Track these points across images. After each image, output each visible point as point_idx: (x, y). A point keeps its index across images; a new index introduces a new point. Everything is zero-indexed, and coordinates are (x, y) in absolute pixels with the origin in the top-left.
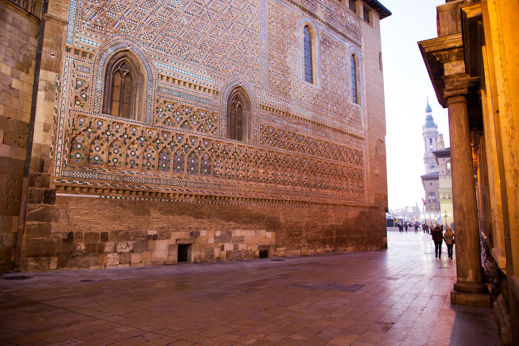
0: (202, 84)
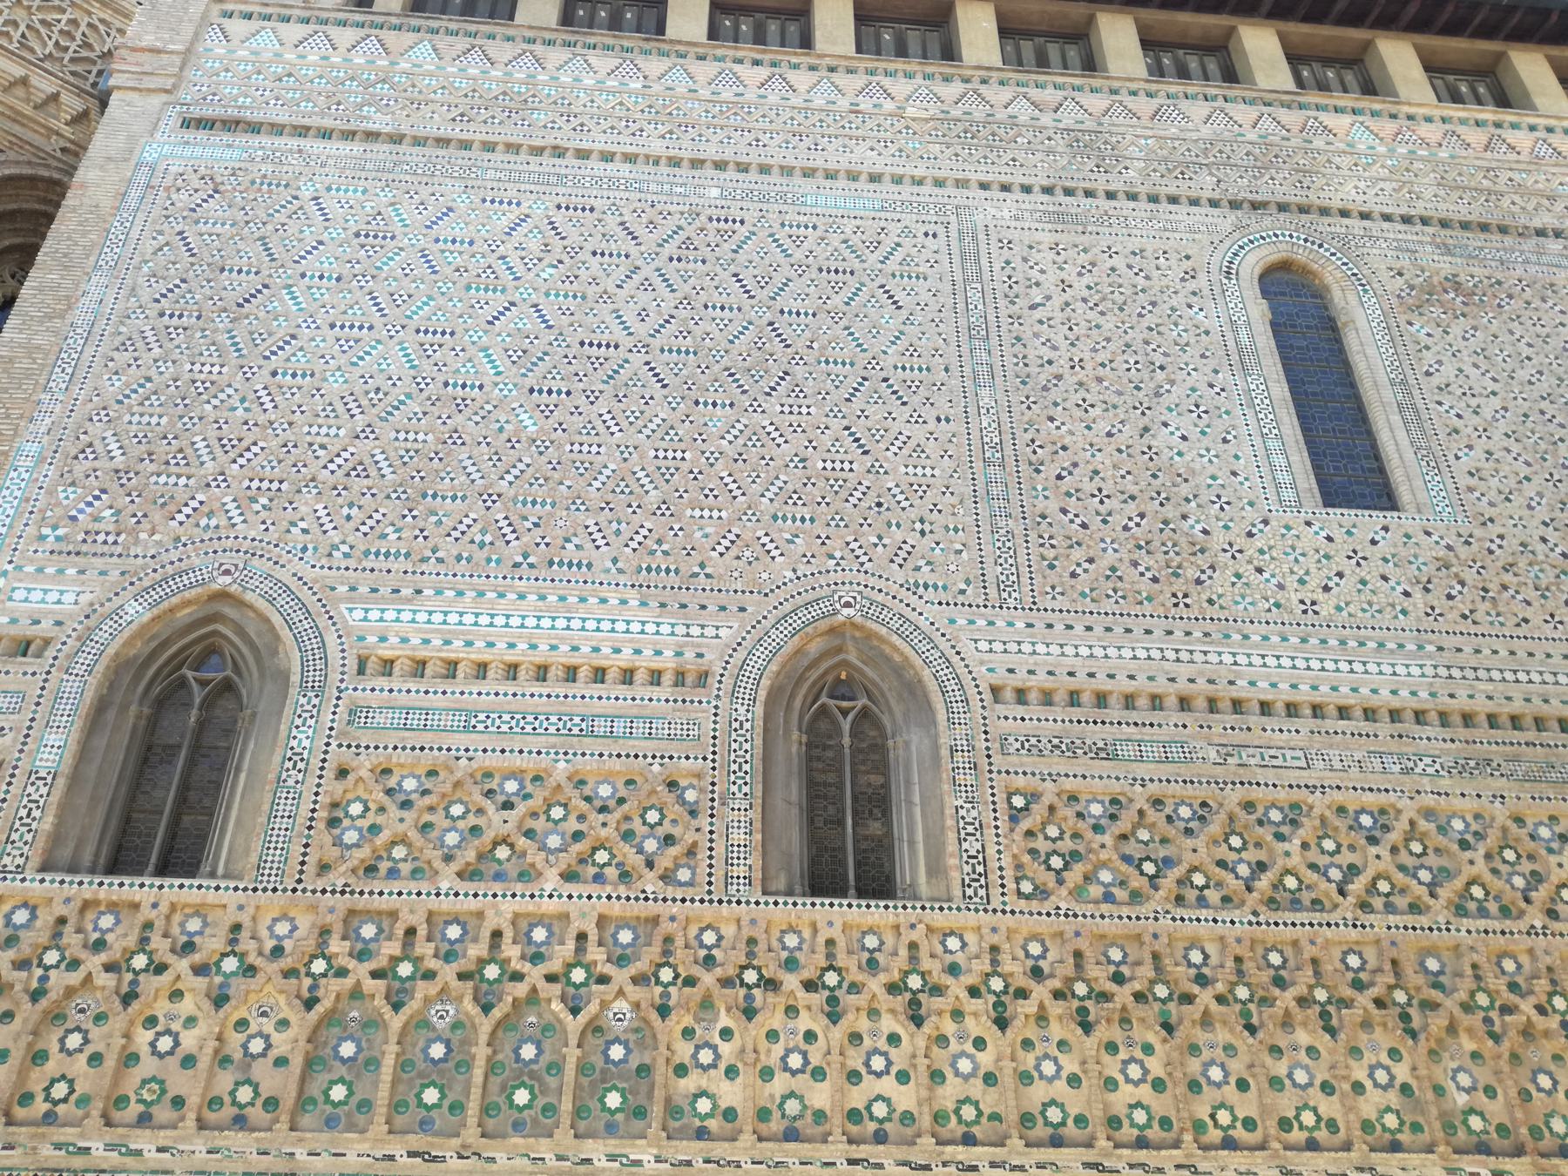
0: (606, 650)
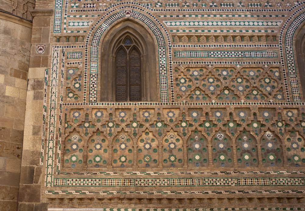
0: (244, 31)
